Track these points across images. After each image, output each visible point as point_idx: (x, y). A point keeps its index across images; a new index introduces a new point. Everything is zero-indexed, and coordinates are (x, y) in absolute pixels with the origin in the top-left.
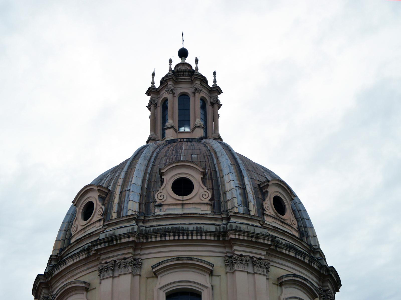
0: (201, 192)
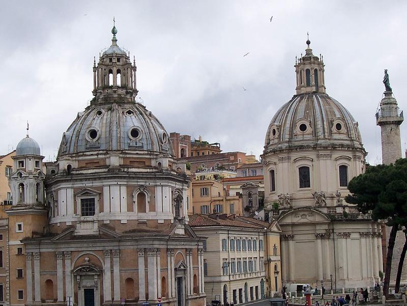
0: (309, 129)
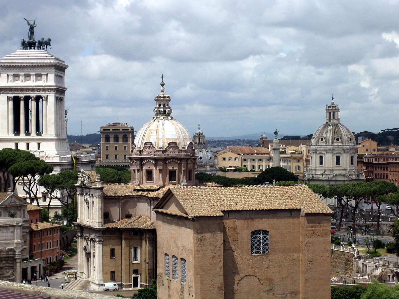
0: (340, 140)
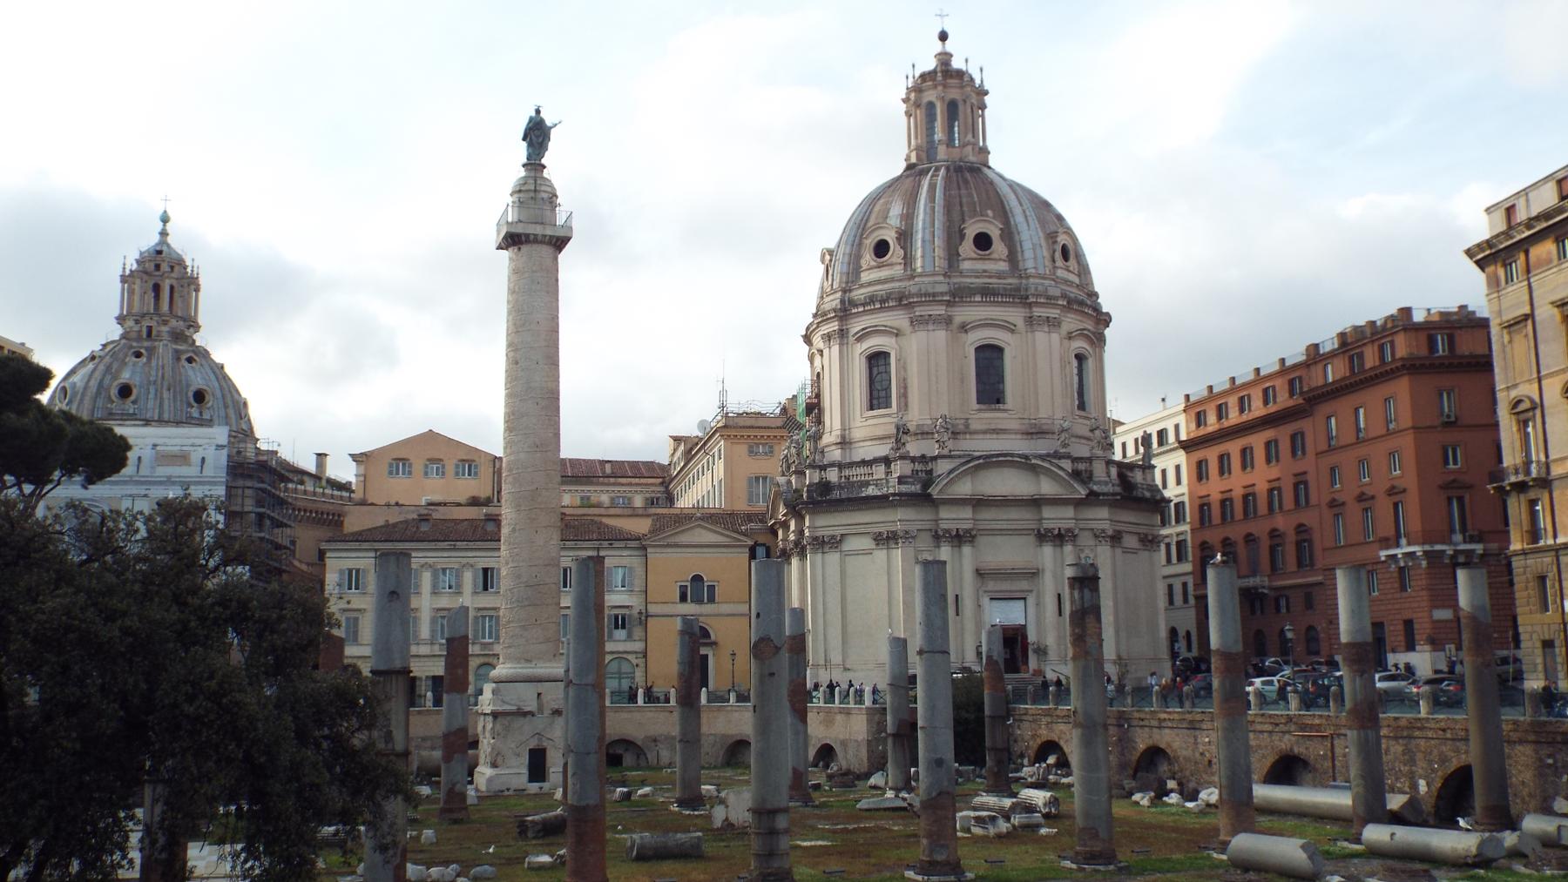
0: (999, 248)
